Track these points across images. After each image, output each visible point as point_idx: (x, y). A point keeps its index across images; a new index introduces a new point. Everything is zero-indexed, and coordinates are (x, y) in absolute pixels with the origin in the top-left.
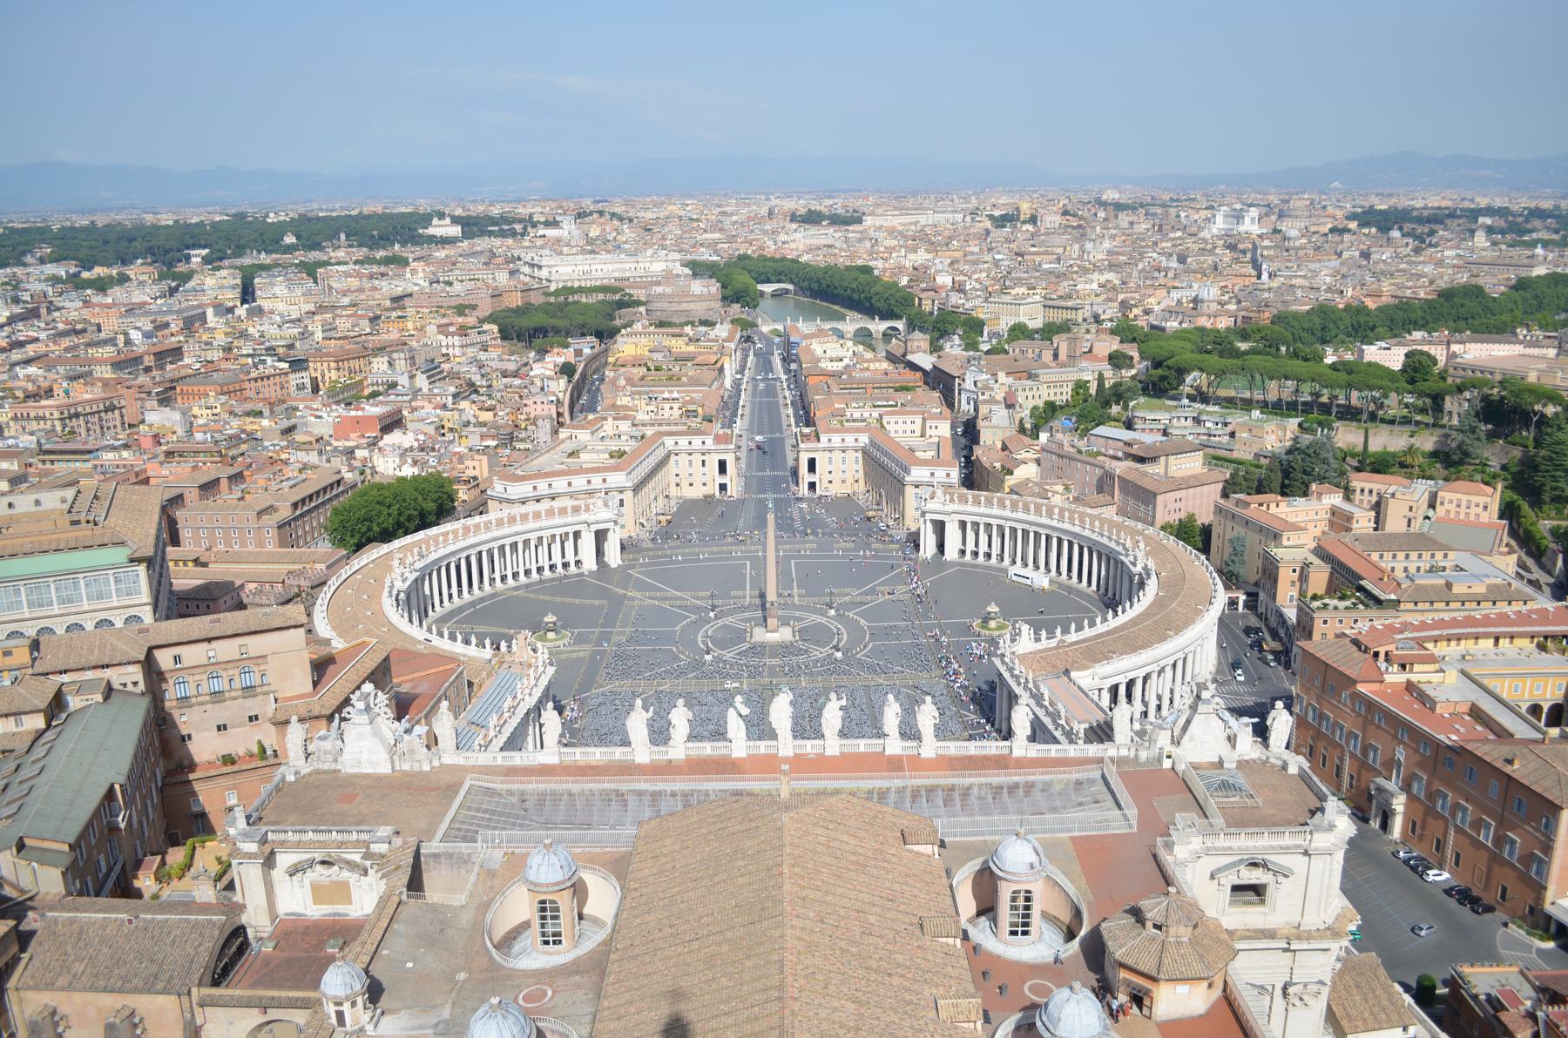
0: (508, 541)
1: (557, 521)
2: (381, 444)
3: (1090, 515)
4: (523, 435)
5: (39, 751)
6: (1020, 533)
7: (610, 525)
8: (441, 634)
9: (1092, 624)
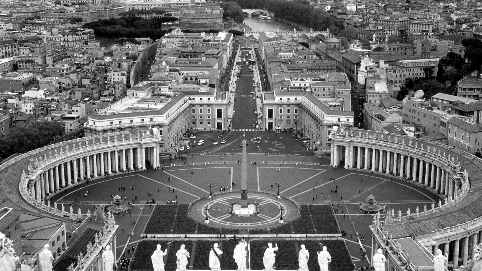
0: (95, 153)
1: (124, 142)
2: (23, 96)
3: (430, 145)
4: (106, 93)
6: (388, 154)
7: (154, 145)
8: (52, 205)
9: (429, 208)
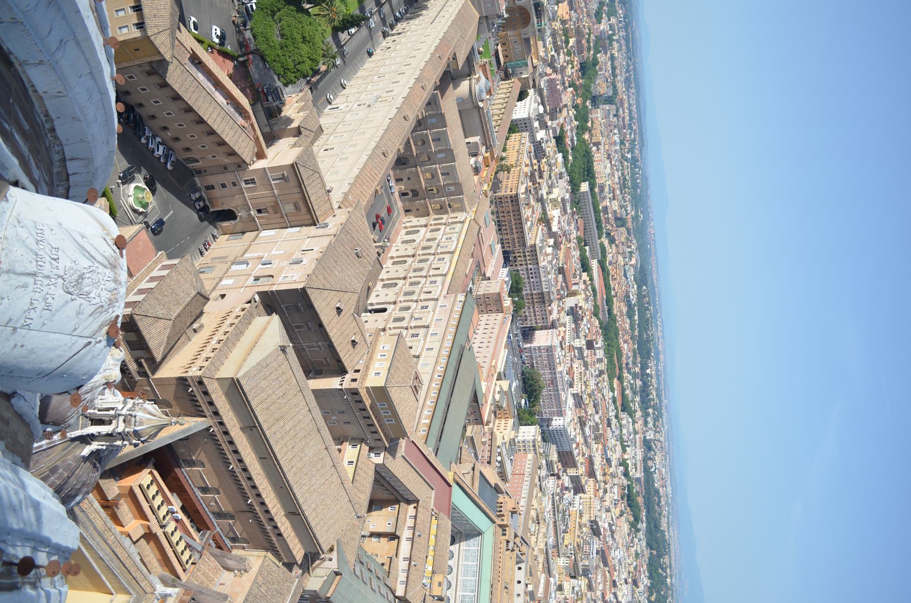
5: (384, 590)
